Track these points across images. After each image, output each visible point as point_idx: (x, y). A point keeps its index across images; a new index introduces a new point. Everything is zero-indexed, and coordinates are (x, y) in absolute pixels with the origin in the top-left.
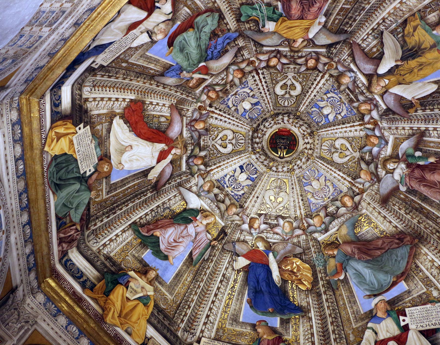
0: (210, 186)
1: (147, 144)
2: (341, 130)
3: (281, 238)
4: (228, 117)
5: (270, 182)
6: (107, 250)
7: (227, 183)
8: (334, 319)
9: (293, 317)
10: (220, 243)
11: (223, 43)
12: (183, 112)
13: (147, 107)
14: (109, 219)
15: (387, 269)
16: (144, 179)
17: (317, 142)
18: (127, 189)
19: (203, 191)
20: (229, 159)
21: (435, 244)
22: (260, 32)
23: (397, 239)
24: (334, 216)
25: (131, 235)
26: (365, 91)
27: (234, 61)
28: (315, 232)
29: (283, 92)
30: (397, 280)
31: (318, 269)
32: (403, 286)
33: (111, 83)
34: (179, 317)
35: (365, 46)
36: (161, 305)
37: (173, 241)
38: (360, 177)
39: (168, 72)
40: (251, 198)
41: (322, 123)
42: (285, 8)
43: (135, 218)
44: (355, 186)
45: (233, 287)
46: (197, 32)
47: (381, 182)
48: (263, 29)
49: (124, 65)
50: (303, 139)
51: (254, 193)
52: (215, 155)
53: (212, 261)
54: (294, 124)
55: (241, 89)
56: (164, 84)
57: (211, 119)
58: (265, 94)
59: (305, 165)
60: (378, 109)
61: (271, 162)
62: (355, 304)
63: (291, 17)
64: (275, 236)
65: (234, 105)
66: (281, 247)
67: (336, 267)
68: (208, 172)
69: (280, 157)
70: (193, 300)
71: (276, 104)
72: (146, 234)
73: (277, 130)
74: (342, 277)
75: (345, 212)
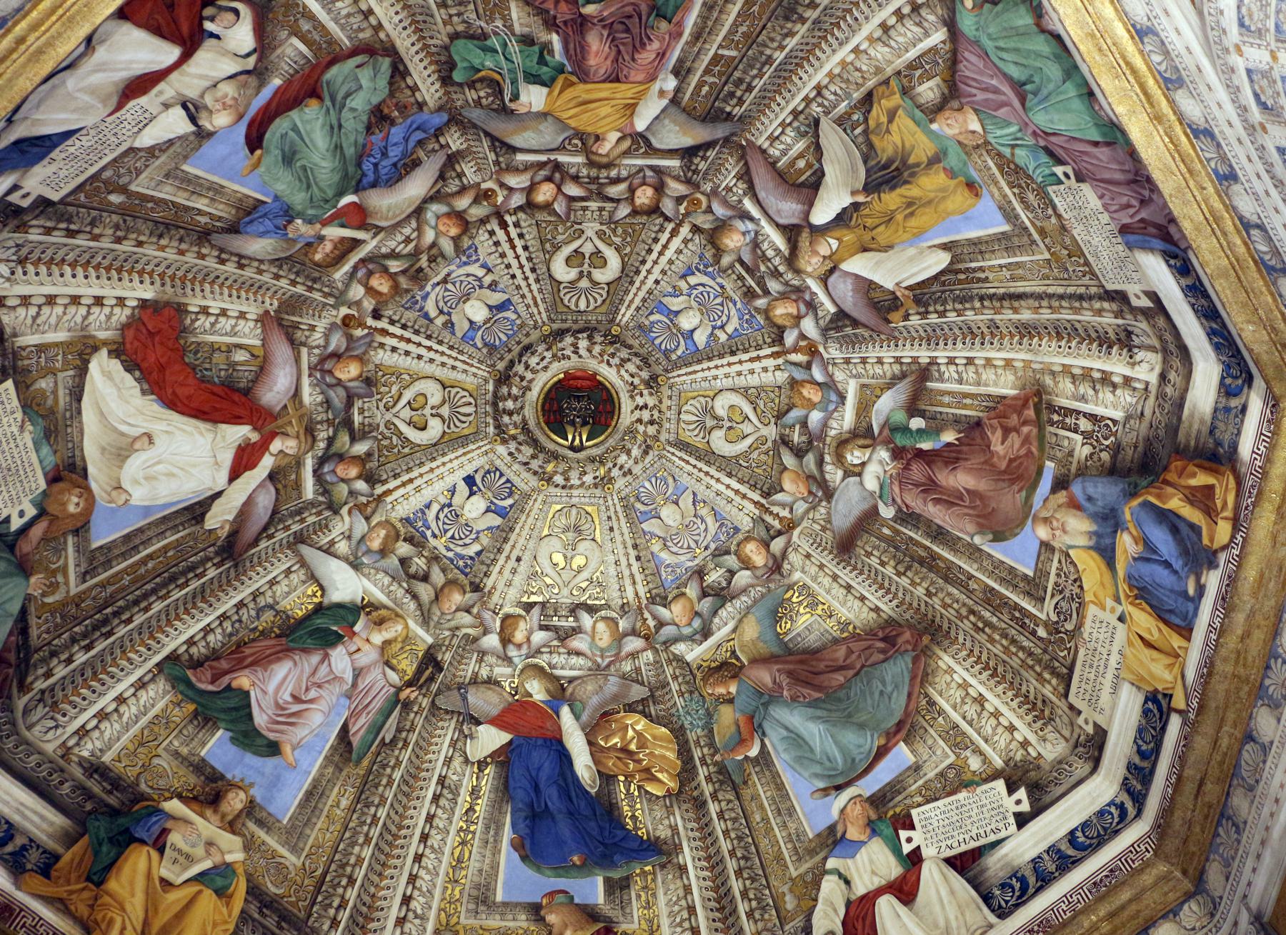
0: (387, 536)
1: (197, 427)
2: (727, 369)
3: (590, 664)
4: (428, 343)
5: (550, 515)
6: (89, 746)
7: (433, 525)
8: (742, 862)
9: (638, 871)
10: (424, 691)
11: (406, 140)
12: (299, 334)
13: (193, 321)
15: (863, 717)
16: (193, 529)
17: (666, 402)
18: (144, 562)
19: (369, 551)
20: (434, 459)
21: (968, 644)
23: (883, 640)
24: (722, 595)
25: (165, 693)
26: (781, 269)
27: (438, 191)
28: (676, 640)
29: (572, 274)
30: (888, 740)
31: (691, 736)
32: (902, 755)
34: (323, 913)
35: (777, 153)
36: (269, 885)
37: (289, 699)
38: (782, 490)
39: (251, 222)
40: (501, 562)
41: (679, 352)
42: (572, 52)
43: (173, 642)
44: (771, 513)
45: (471, 809)
47: (836, 497)
48: (513, 106)
50: (632, 397)
51: (507, 547)
52: (396, 450)
53: (406, 744)
54: (606, 357)
55: (459, 267)
56: (241, 256)
57: (381, 352)
58: (526, 279)
59: (640, 466)
60: (816, 315)
61: (549, 462)
62: (790, 815)
63: (587, 74)
64: (574, 660)
65: (441, 312)
66: (589, 688)
67: (738, 726)
68: (380, 499)
69: (572, 448)
71: (555, 305)
72: (211, 688)
73: (562, 376)
74: (754, 752)
75: (749, 581)
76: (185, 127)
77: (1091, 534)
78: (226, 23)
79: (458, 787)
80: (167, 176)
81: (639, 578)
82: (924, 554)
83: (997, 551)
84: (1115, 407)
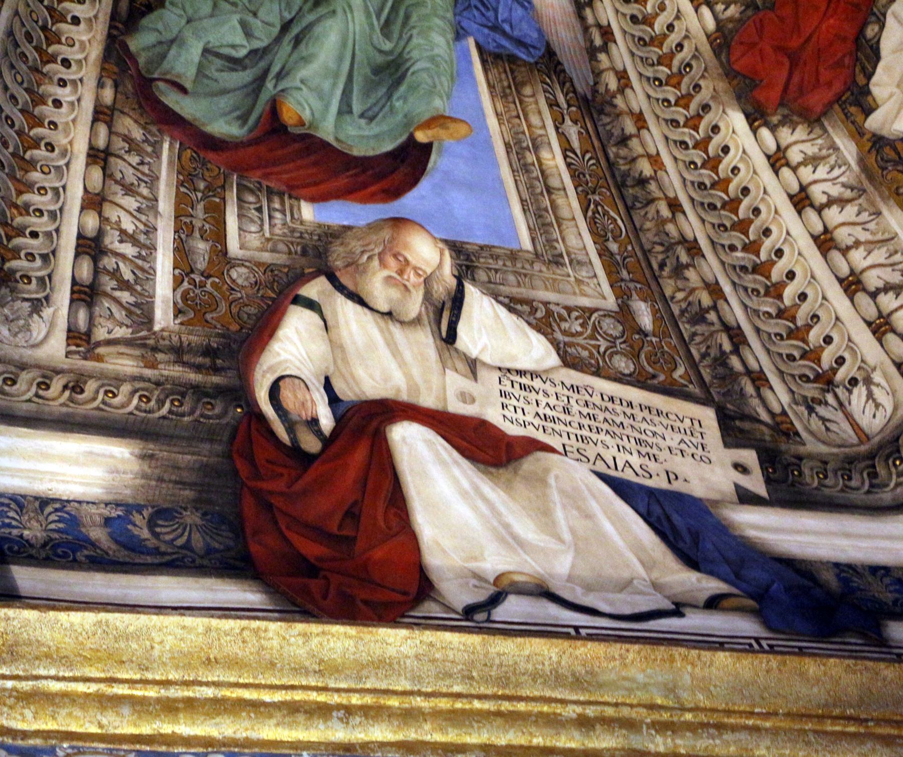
33: (753, 303)
39: (520, 43)
46: (276, 69)
49: (645, 317)
78: (301, 394)
80: (556, 261)
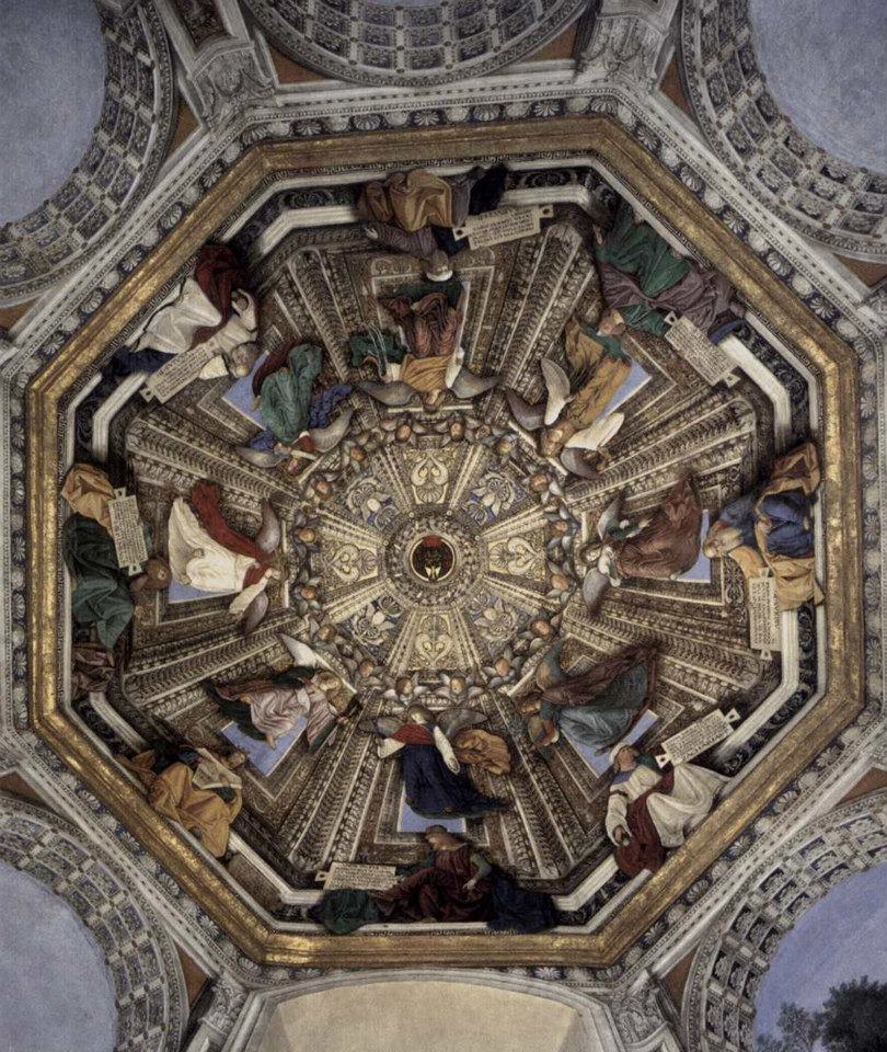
4: (348, 524)
13: (227, 495)
14: (165, 666)
21: (681, 645)
22: (380, 383)
24: (525, 655)
28: (500, 685)
31: (516, 739)
32: (650, 717)
38: (553, 588)
40: (395, 648)
44: (548, 604)
48: (383, 378)
53: (341, 749)
56: (251, 464)
64: (440, 701)
68: (325, 613)
70: (312, 808)
76: (223, 372)
77: (738, 538)
79: (372, 772)
81: (475, 652)
82: (643, 600)
83: (685, 579)
84: (735, 457)
